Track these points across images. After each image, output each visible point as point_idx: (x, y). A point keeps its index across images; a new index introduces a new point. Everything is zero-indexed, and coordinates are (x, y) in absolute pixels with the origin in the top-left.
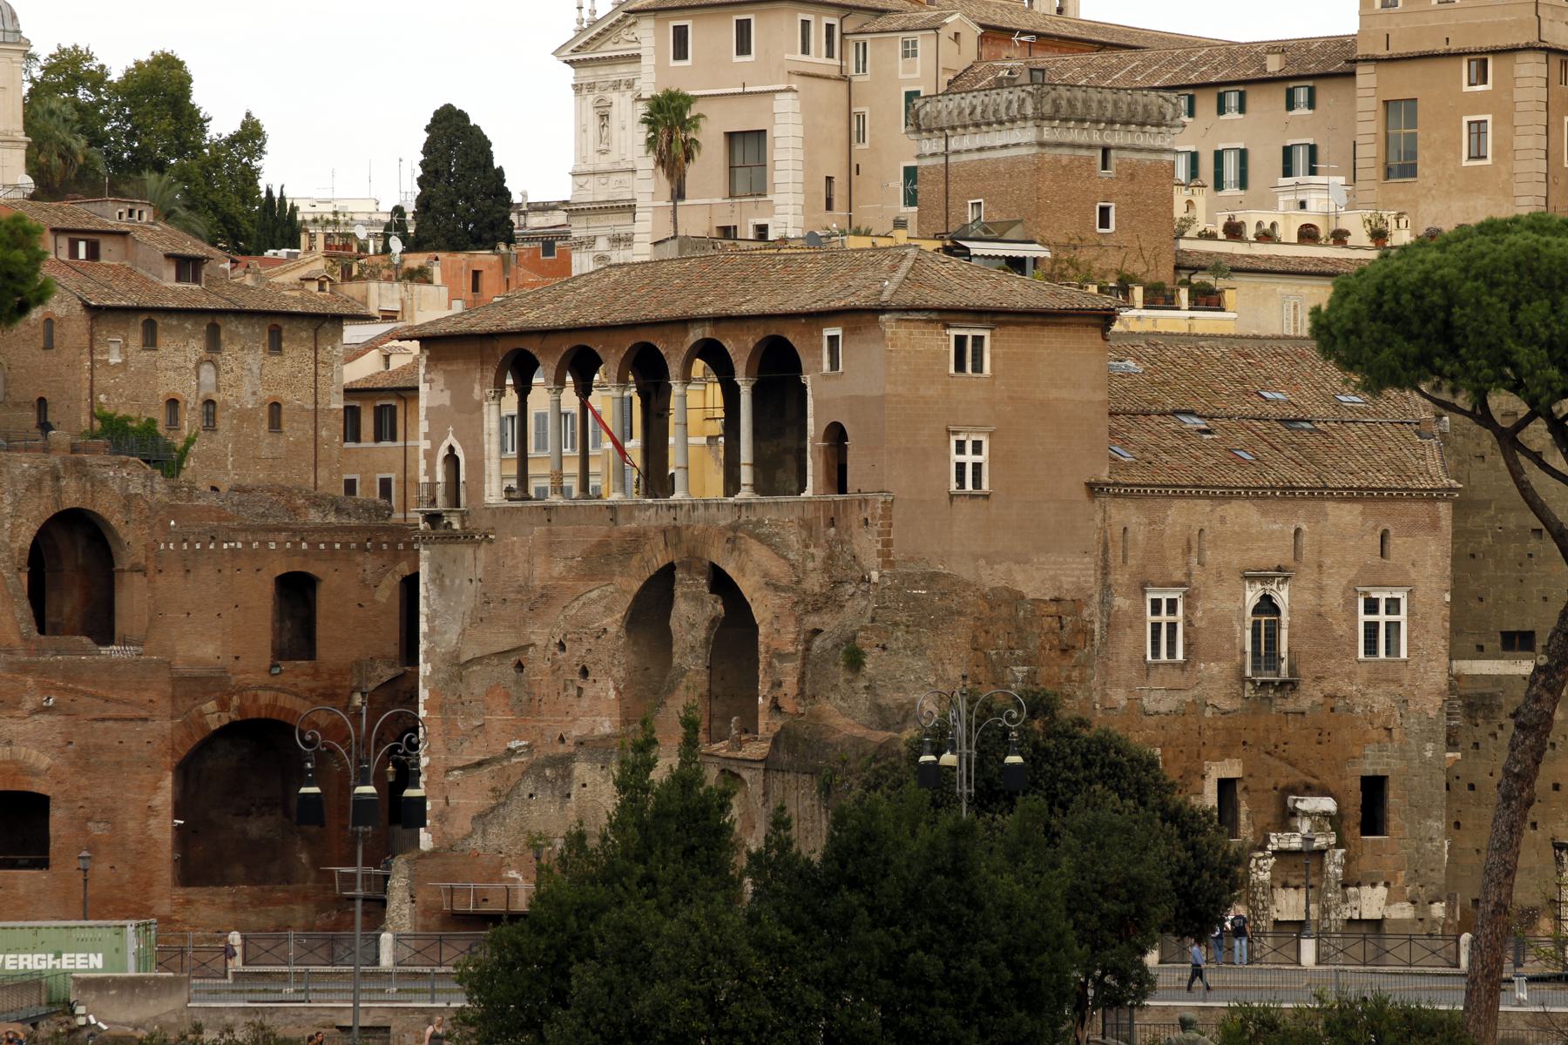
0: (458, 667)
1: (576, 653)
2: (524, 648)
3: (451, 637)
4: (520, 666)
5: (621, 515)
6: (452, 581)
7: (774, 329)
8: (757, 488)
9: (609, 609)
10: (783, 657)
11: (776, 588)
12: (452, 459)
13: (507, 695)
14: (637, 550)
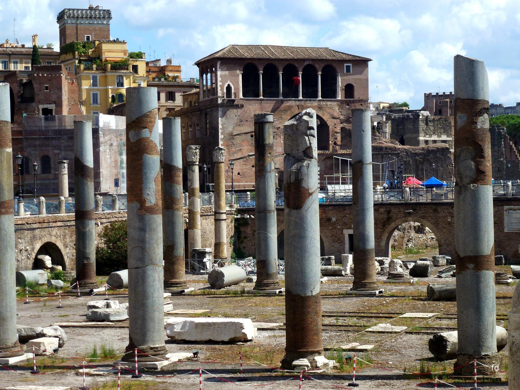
0: (232, 136)
3: (230, 129)
6: (230, 116)
7: (329, 63)
10: (337, 133)
11: (334, 118)
12: (229, 88)
13: (248, 142)
14: (289, 110)
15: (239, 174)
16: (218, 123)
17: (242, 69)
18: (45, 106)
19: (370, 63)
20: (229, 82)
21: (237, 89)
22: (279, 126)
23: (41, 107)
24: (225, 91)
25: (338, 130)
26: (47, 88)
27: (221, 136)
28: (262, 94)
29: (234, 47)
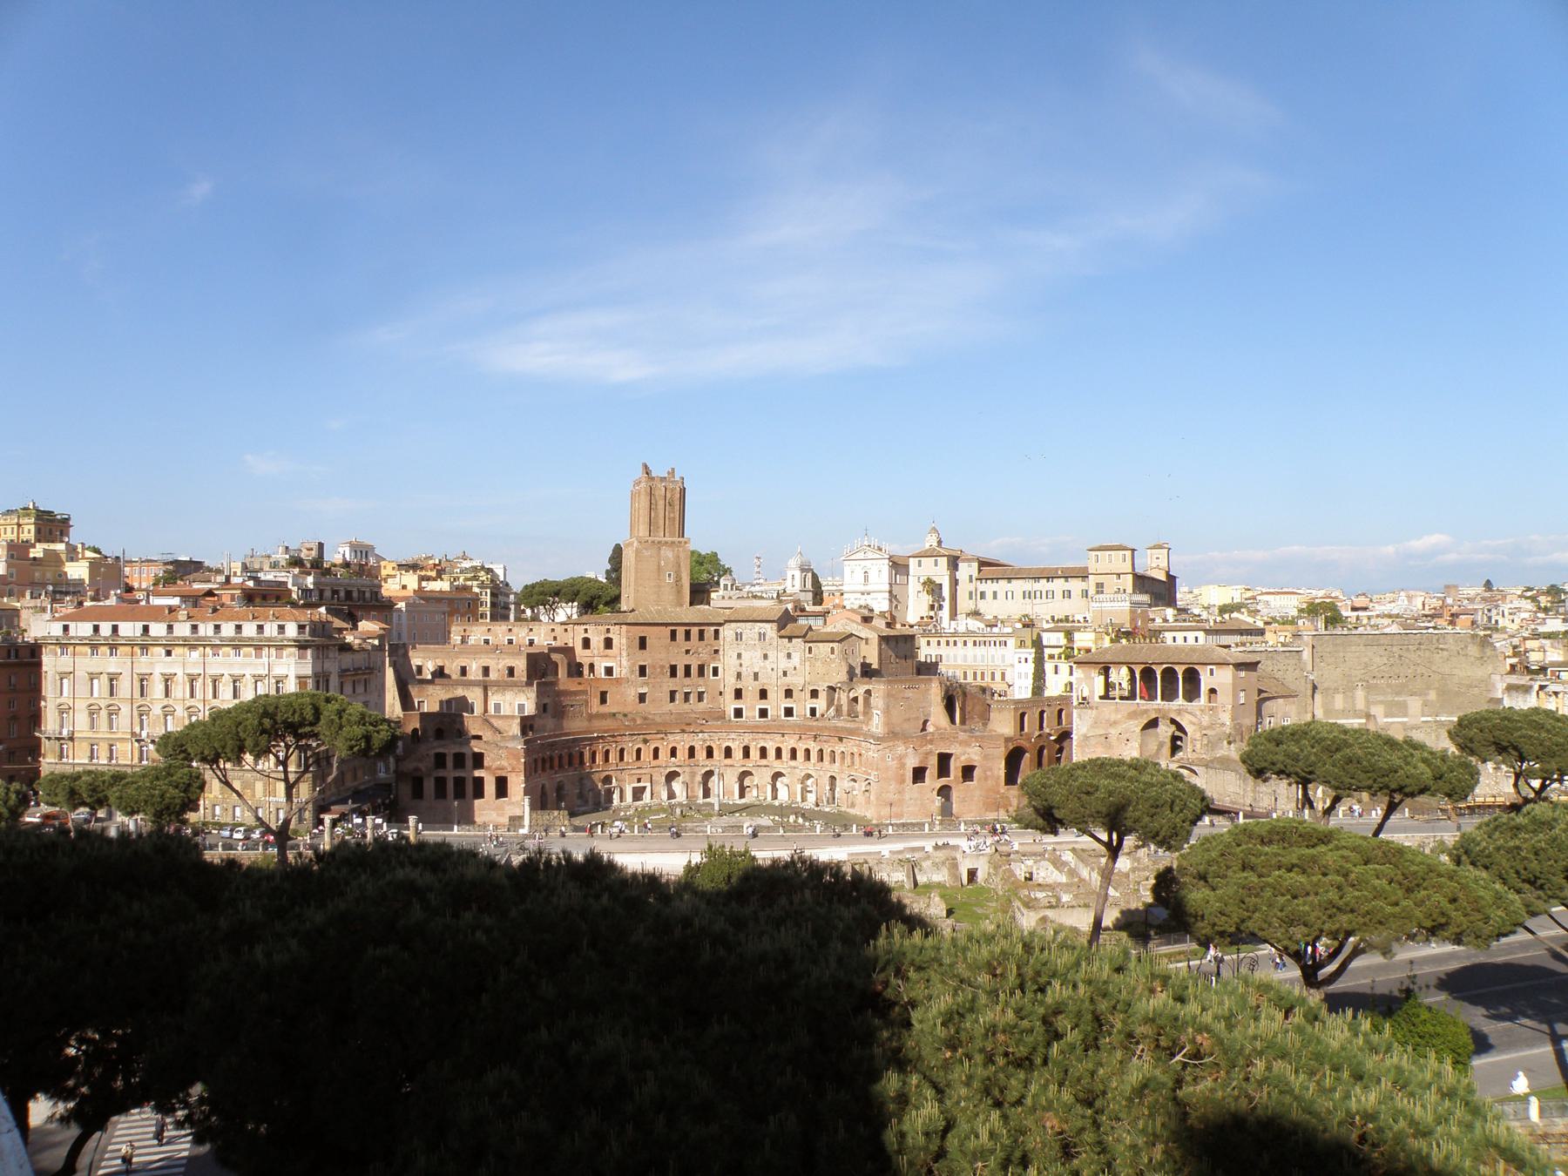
0: (1086, 738)
1: (1125, 736)
3: (1084, 730)
25: (1198, 736)
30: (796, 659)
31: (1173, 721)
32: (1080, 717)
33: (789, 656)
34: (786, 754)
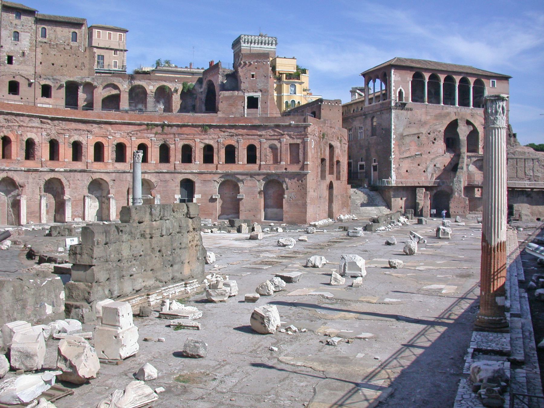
0: (402, 137)
1: (432, 136)
2: (419, 133)
3: (401, 130)
4: (418, 137)
5: (444, 108)
8: (473, 106)
9: (441, 127)
12: (400, 93)
15: (407, 171)
16: (391, 124)
17: (412, 76)
18: (251, 94)
19: (510, 79)
20: (401, 88)
21: (407, 94)
22: (440, 129)
23: (247, 95)
24: (398, 95)
26: (253, 76)
27: (393, 136)
28: (427, 100)
29: (399, 59)
30: (25, 41)
31: (468, 123)
32: (397, 117)
33: (16, 36)
34: (109, 153)
